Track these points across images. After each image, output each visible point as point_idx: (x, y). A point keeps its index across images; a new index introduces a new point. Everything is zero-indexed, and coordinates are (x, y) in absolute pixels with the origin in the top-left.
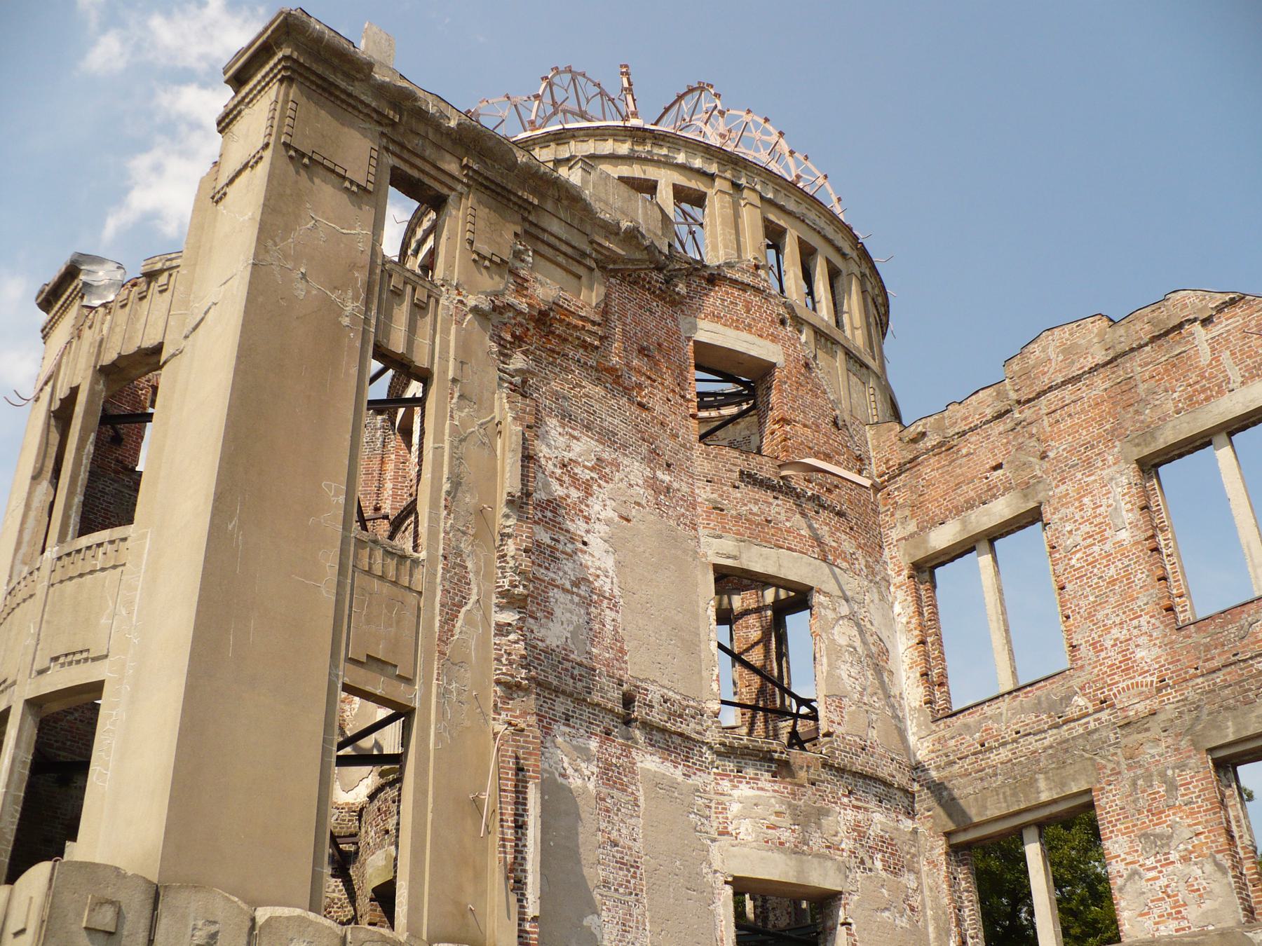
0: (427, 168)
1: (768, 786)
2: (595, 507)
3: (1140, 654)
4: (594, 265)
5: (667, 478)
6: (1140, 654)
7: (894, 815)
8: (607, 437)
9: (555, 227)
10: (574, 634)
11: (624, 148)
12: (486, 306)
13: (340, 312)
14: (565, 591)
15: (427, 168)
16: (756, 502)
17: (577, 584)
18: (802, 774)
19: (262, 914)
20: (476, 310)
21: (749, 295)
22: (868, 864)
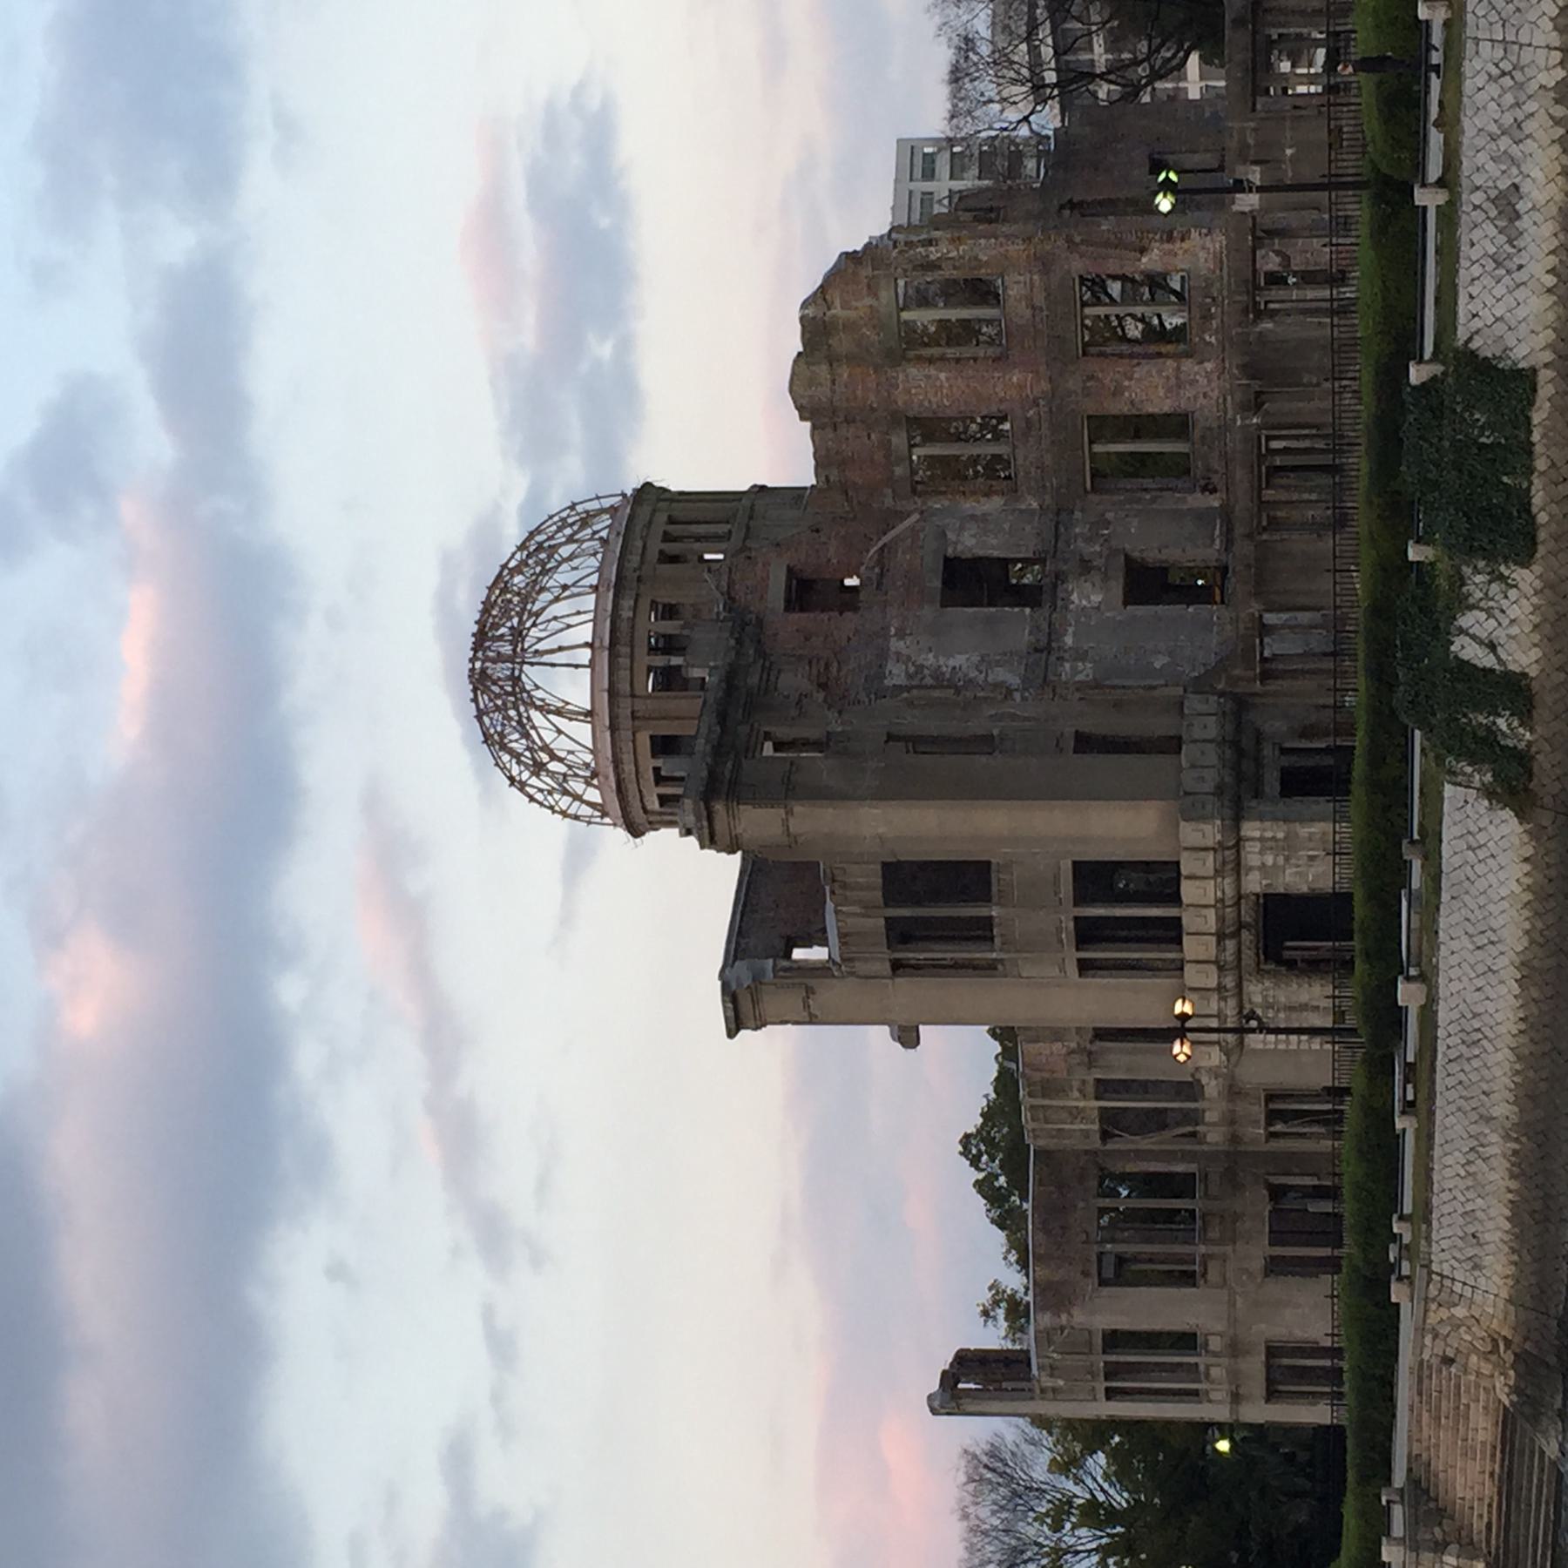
3: (1015, 379)
6: (1015, 379)
9: (753, 680)
11: (625, 650)
15: (754, 739)
17: (981, 672)
19: (1184, 763)
21: (737, 577)
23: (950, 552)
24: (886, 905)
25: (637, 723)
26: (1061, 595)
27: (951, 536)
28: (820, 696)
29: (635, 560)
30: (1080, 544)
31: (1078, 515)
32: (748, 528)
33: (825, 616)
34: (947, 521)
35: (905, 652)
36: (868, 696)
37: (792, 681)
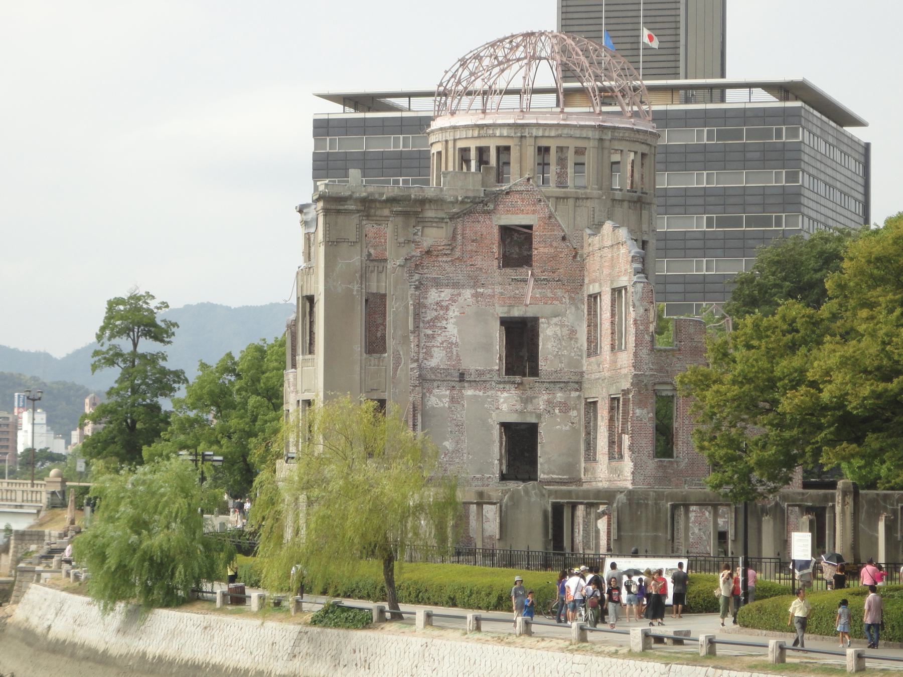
0: (378, 218)
1: (513, 392)
2: (450, 313)
4: (448, 220)
5: (482, 290)
7: (568, 392)
8: (456, 285)
10: (441, 360)
12: (402, 264)
13: (352, 290)
14: (438, 347)
16: (518, 289)
17: (441, 344)
18: (527, 386)
20: (399, 266)
22: (552, 411)
23: (541, 320)
24: (303, 297)
25: (444, 143)
26: (507, 386)
27: (555, 320)
28: (417, 253)
29: (535, 132)
30: (546, 397)
31: (574, 394)
32: (567, 198)
33: (495, 249)
34: (570, 316)
35: (461, 299)
36: (417, 280)
37: (434, 236)
